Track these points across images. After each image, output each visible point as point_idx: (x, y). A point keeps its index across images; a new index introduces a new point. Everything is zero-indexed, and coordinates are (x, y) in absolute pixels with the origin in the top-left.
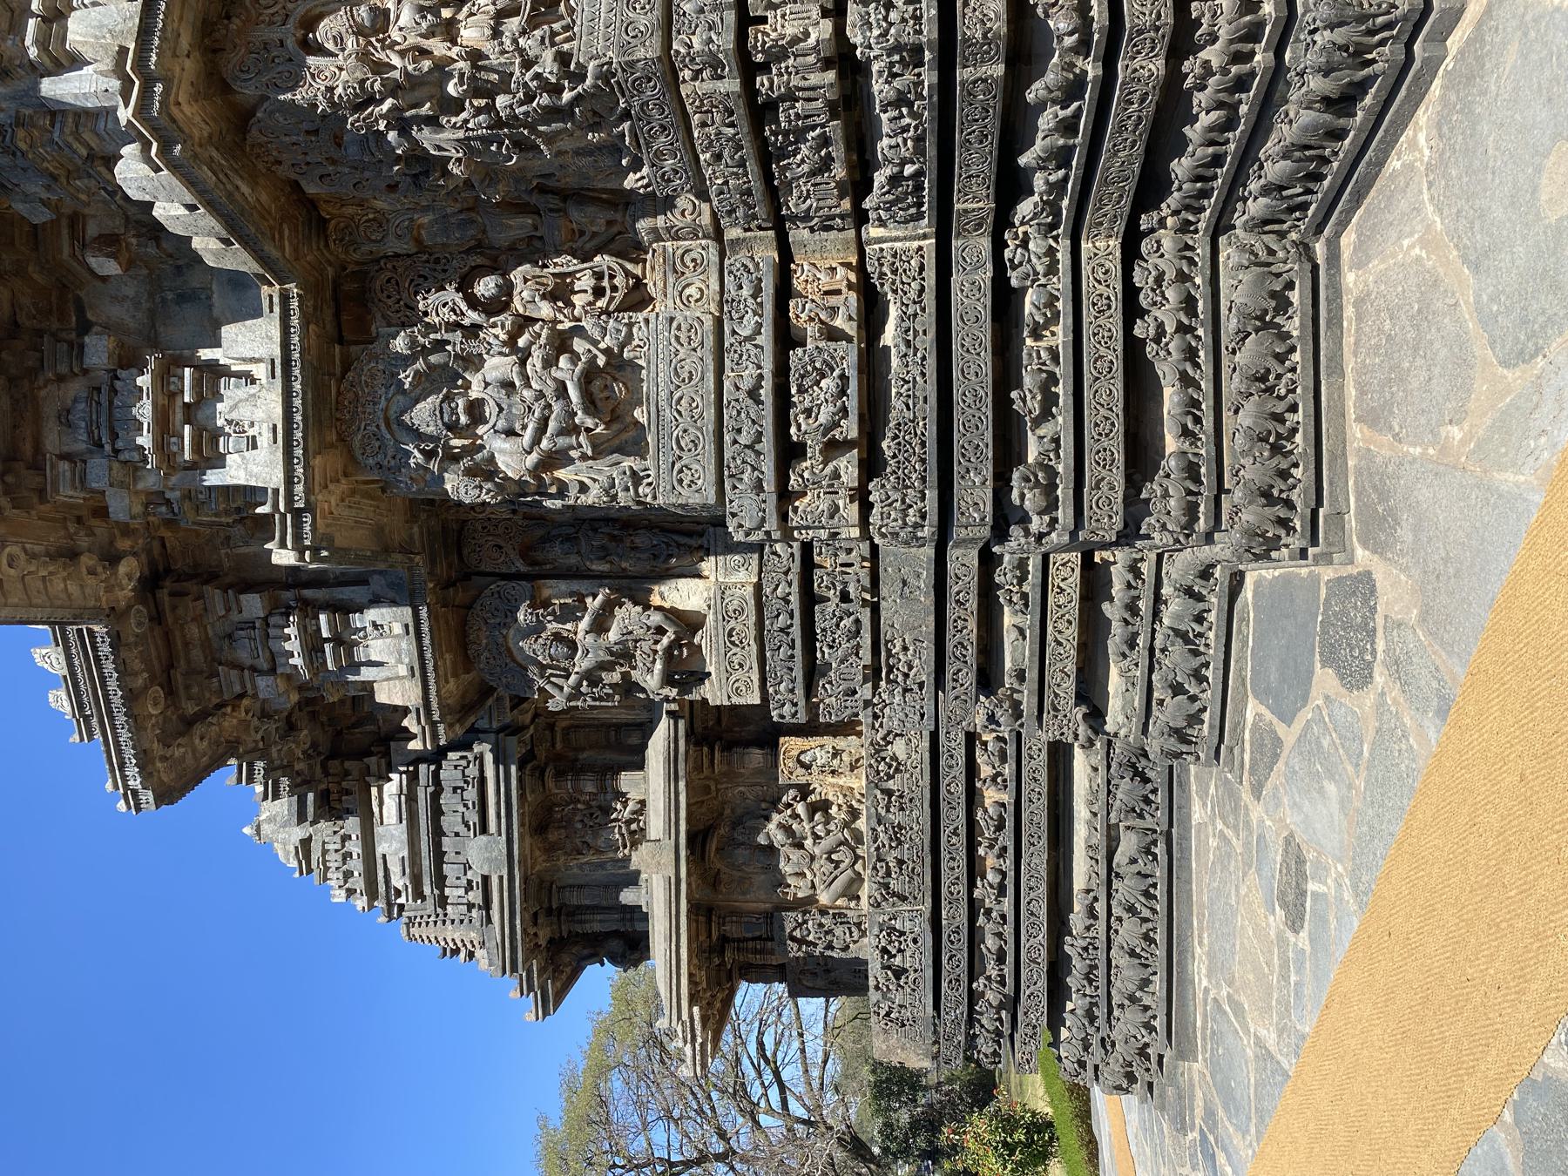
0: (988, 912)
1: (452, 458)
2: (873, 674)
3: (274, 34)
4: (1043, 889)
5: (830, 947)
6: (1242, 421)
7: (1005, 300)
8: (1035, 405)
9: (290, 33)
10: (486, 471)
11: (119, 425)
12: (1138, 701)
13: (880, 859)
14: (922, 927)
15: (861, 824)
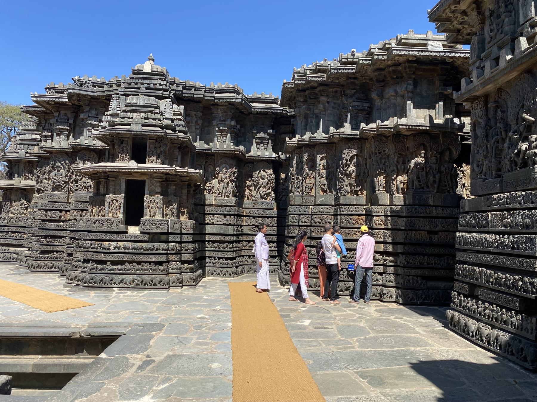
0: (7, 234)
1: (53, 167)
2: (34, 218)
3: (87, 156)
4: (9, 243)
5: (4, 209)
6: (42, 263)
7: (61, 237)
8: (47, 240)
9: (87, 158)
10: (51, 171)
11: (61, 123)
12: (27, 255)
13: (16, 218)
14: (5, 223)
15: (23, 215)
